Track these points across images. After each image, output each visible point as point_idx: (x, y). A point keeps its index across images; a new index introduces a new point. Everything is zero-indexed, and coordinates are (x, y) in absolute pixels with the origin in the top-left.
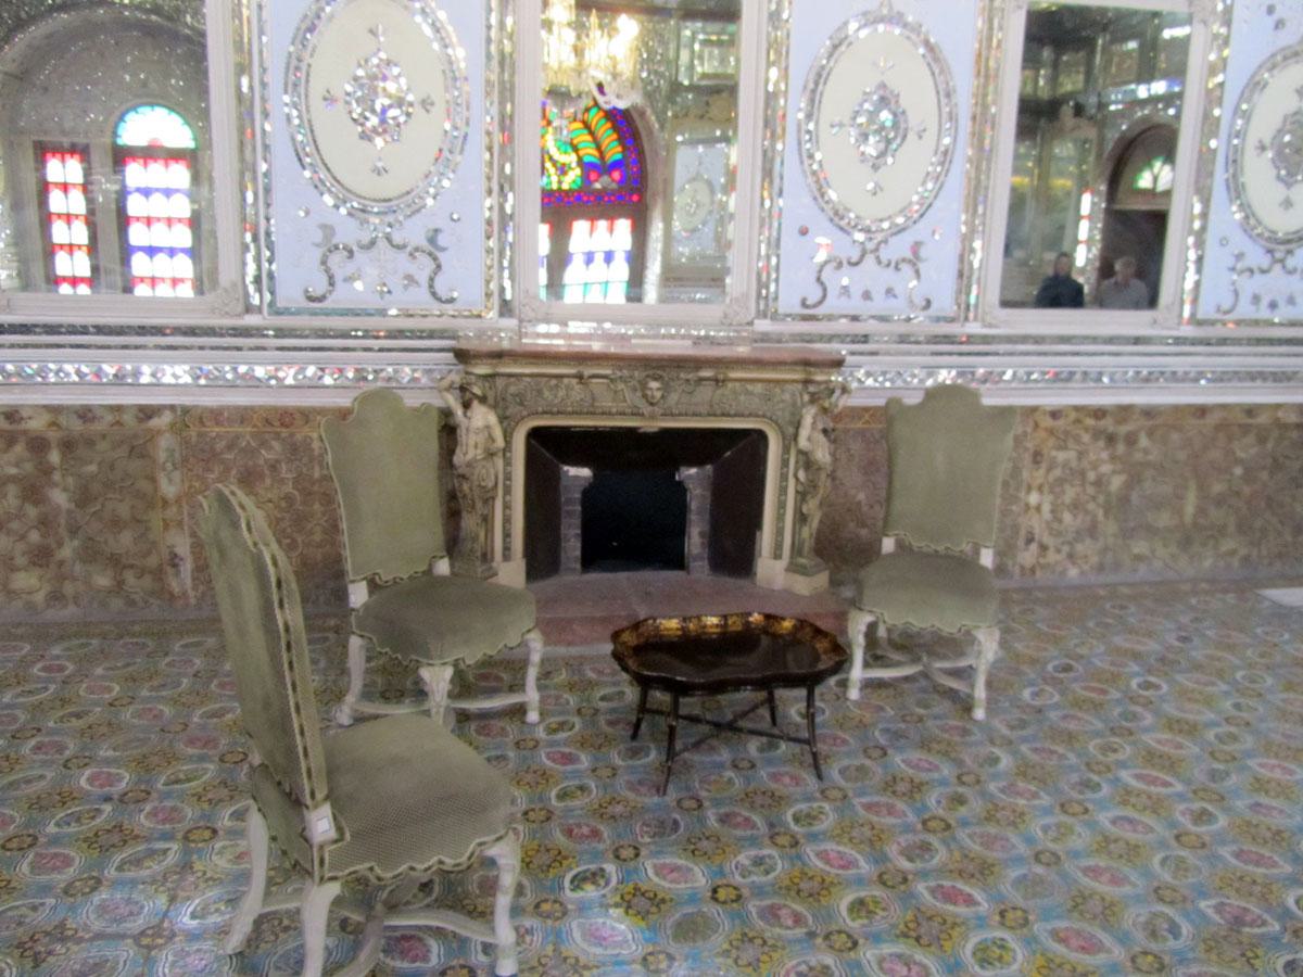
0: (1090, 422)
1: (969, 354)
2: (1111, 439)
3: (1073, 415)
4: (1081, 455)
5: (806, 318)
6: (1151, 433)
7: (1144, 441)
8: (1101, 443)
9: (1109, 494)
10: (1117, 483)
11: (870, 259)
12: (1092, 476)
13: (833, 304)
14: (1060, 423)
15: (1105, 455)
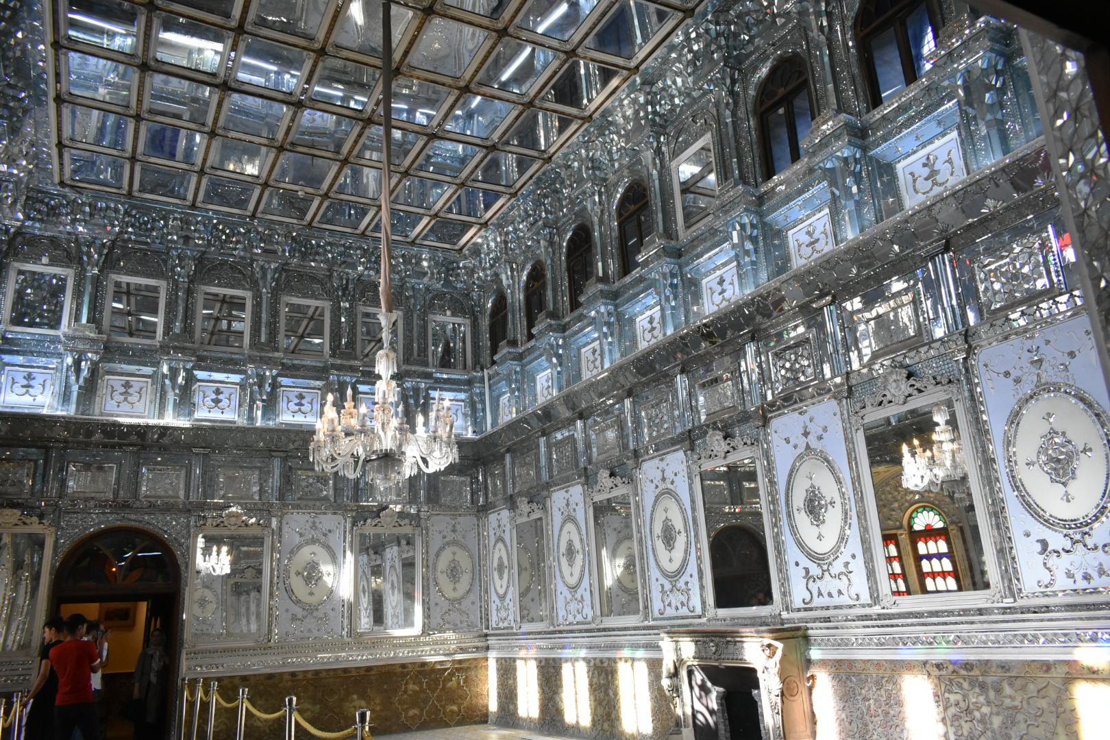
0: (963, 672)
1: (883, 626)
2: (983, 686)
3: (951, 668)
4: (965, 697)
5: (806, 610)
6: (1011, 685)
7: (1008, 690)
8: (977, 690)
9: (993, 731)
10: (997, 721)
11: (826, 573)
12: (977, 714)
13: (817, 602)
14: (944, 672)
15: (982, 699)
